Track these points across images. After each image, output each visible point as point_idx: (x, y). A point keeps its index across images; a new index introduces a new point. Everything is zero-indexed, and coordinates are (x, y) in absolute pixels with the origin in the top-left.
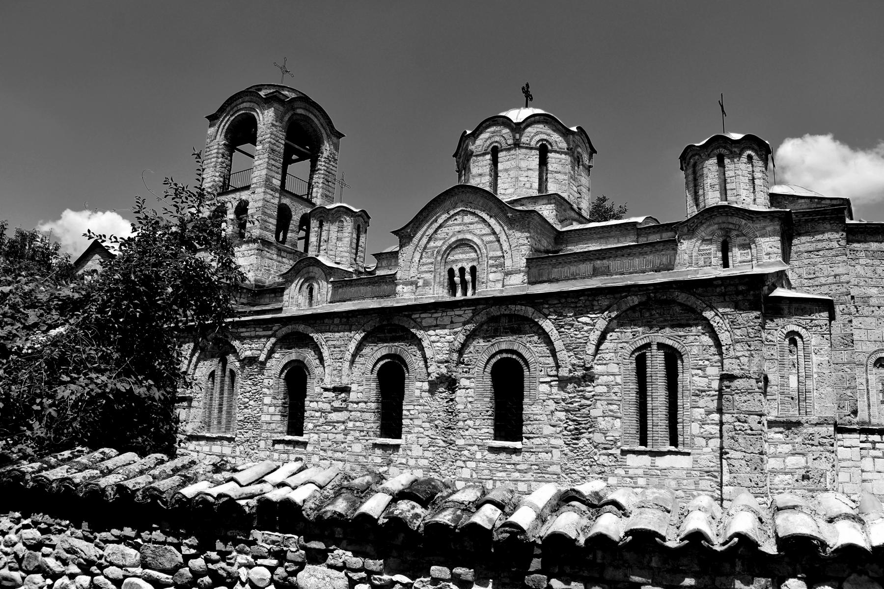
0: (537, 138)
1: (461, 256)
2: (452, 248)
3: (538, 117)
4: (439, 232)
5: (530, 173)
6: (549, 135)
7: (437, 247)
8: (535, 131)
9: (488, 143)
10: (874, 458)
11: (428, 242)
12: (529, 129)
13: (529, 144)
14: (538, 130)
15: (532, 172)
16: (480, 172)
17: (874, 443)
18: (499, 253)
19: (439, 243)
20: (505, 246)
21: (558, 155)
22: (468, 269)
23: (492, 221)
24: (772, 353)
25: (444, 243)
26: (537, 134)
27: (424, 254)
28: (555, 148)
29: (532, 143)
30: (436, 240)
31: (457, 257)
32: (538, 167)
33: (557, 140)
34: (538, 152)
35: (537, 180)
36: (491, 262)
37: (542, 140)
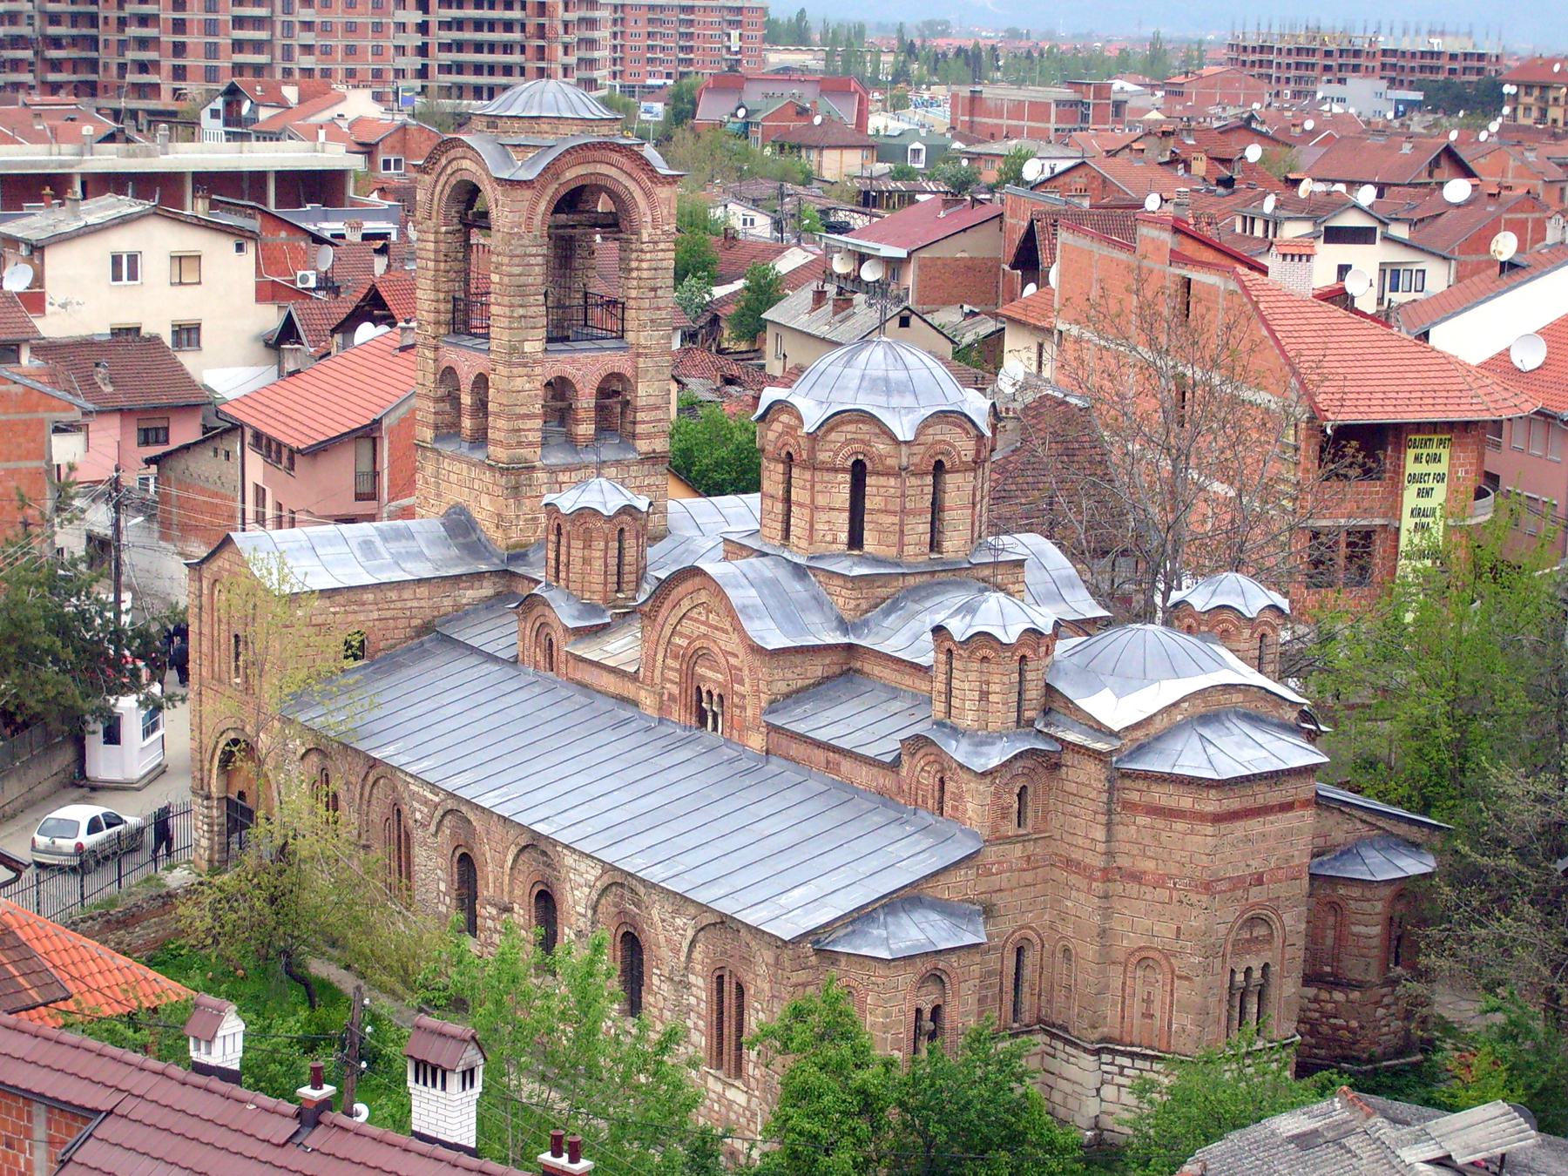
1: (710, 674)
10: (1120, 1086)
12: (833, 436)
17: (1122, 1068)
21: (882, 480)
28: (880, 468)
32: (847, 505)
34: (848, 477)
35: (846, 527)
37: (857, 453)
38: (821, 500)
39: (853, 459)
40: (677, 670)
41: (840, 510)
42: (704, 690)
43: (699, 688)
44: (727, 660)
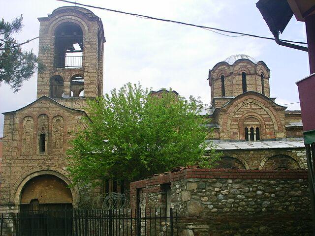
1: (251, 123)
2: (247, 119)
7: (239, 118)
18: (270, 123)
20: (274, 121)
22: (255, 129)
23: (267, 109)
31: (248, 123)
36: (267, 127)
40: (237, 125)
42: (249, 128)
43: (246, 129)
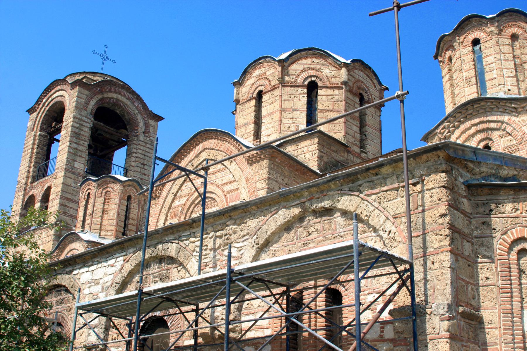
0: (305, 75)
3: (305, 52)
4: (184, 187)
5: (296, 114)
6: (319, 70)
7: (179, 206)
8: (302, 68)
9: (254, 88)
11: (173, 201)
13: (295, 82)
14: (306, 66)
15: (298, 113)
16: (245, 121)
19: (183, 201)
21: (330, 91)
24: (487, 276)
25: (187, 200)
26: (304, 70)
27: (169, 215)
29: (298, 82)
30: (181, 197)
32: (305, 107)
33: (329, 75)
34: (305, 90)
38: (287, 105)
39: (309, 80)
41: (301, 111)
44: (223, 191)
